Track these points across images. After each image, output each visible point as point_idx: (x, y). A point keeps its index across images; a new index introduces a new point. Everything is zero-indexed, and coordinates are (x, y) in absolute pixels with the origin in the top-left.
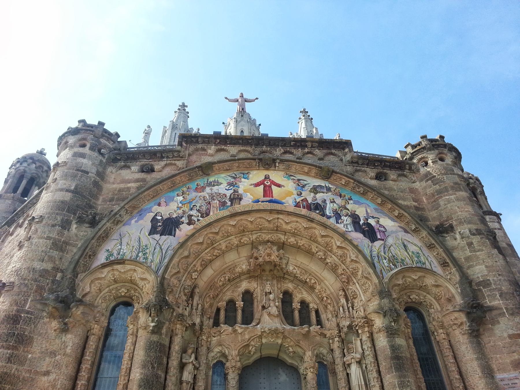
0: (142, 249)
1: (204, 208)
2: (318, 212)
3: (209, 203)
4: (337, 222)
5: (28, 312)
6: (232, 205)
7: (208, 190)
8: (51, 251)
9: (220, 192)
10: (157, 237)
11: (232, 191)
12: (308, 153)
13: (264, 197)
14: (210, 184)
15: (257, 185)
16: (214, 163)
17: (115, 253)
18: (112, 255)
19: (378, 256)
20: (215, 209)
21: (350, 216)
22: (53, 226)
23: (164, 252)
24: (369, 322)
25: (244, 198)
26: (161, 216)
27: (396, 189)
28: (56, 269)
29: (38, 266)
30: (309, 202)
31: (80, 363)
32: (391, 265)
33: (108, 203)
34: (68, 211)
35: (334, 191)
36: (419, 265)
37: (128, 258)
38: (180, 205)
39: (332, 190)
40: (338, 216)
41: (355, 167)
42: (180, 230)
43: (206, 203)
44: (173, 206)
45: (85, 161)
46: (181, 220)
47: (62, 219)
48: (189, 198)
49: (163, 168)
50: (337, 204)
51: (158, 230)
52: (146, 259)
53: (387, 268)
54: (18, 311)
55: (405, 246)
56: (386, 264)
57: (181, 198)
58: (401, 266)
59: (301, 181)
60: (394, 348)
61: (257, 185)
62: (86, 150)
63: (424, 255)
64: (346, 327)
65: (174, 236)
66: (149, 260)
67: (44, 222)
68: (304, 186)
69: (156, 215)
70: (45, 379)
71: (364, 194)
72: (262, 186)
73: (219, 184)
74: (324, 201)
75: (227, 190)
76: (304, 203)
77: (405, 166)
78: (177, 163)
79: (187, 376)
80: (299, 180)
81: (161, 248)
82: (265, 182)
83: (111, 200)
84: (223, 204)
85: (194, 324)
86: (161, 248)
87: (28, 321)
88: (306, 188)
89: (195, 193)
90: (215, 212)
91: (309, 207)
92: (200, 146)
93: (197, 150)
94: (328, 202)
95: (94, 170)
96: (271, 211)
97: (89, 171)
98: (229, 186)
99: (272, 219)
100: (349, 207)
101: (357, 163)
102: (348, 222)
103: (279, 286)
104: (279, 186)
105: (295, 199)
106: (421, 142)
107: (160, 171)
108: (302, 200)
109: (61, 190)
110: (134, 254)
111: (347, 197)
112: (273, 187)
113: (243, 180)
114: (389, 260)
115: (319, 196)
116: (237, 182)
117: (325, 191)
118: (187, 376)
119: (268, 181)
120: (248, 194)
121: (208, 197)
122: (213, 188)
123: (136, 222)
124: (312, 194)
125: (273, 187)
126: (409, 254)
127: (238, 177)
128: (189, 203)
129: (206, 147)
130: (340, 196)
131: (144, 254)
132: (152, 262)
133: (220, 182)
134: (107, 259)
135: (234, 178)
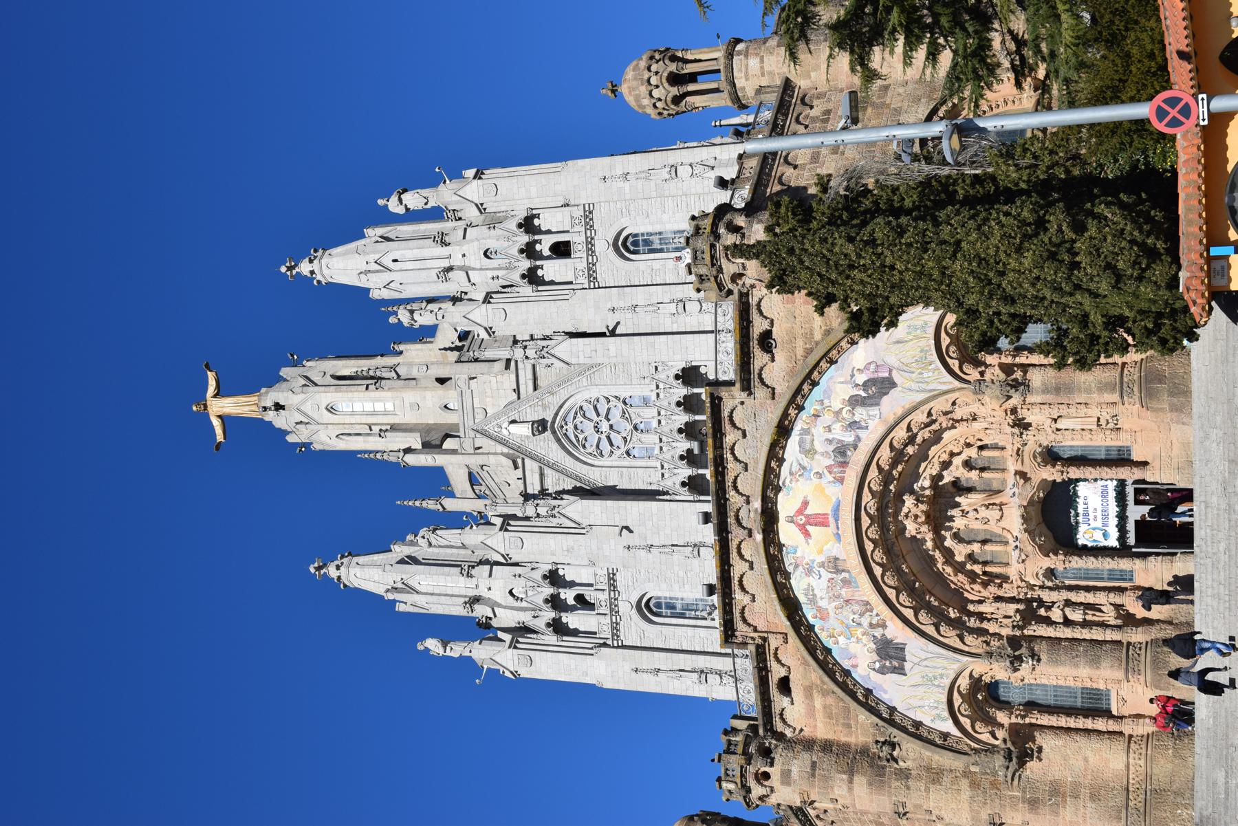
0: (929, 681)
1: (856, 608)
2: (849, 453)
3: (847, 601)
4: (867, 428)
5: (1024, 792)
6: (848, 571)
7: (823, 604)
8: (944, 783)
9: (826, 587)
10: (907, 666)
11: (822, 570)
12: (733, 453)
13: (829, 526)
14: (813, 600)
15: (807, 534)
16: (779, 597)
17: (935, 712)
18: (939, 715)
19: (918, 382)
20: (857, 593)
21: (853, 409)
22: (908, 788)
23: (930, 655)
24: (1014, 411)
25: (833, 555)
26: (875, 663)
27: (790, 325)
28: (967, 774)
29: (966, 793)
30: (833, 463)
31: (1068, 730)
32: (930, 368)
33: (853, 729)
34: (883, 775)
35: (807, 423)
36: (931, 331)
37: (944, 698)
38: (853, 639)
39: (806, 427)
40: (853, 425)
41: (756, 383)
42: (896, 637)
43: (847, 605)
44: (855, 648)
45: (795, 771)
46: (879, 637)
47: (897, 780)
48: (839, 629)
49: (783, 665)
50: (833, 423)
51: (897, 665)
52: (942, 676)
53: (937, 372)
54: (1024, 802)
55: (898, 342)
56: (930, 374)
57: (841, 639)
58: (932, 355)
59: (793, 470)
60: (1046, 391)
61: (807, 534)
62: (775, 771)
63: (912, 319)
64: (1013, 430)
65: (906, 644)
66: (944, 672)
67: (905, 800)
68: (804, 468)
69: (874, 669)
70: (1091, 760)
71: (815, 384)
72: (808, 527)
73: (809, 589)
74: (830, 441)
75: (820, 576)
76: (835, 470)
77: (743, 303)
78: (772, 648)
79: (1076, 616)
80: (791, 473)
81: (925, 659)
82: (801, 522)
83: (849, 726)
84: (846, 583)
85: (1018, 611)
86: (925, 659)
87: (1034, 789)
88: (806, 464)
89: (831, 621)
90: (860, 593)
91: (844, 464)
92: (737, 614)
93: (744, 620)
94: (830, 436)
95: (806, 755)
96: (858, 519)
97: (809, 762)
98: (814, 575)
99: (867, 519)
100: (837, 404)
101: (749, 381)
102: (864, 413)
103: (948, 495)
104: (805, 504)
105: (829, 482)
106: (696, 275)
107: (789, 668)
108: (830, 473)
109: (851, 789)
110: (936, 690)
111: (818, 408)
112: (809, 511)
113: (799, 554)
114: (923, 368)
115: (819, 446)
116: (804, 562)
117: (808, 438)
118: (1076, 616)
119: (799, 518)
120: (825, 548)
121: (837, 603)
122: (818, 597)
123: (886, 692)
124: (817, 457)
125: (809, 511)
126: (912, 340)
127: (794, 561)
128: (848, 628)
129: (740, 607)
130: (816, 416)
131: (935, 678)
132: (946, 668)
133: (806, 587)
134: (944, 720)
135: (797, 566)
